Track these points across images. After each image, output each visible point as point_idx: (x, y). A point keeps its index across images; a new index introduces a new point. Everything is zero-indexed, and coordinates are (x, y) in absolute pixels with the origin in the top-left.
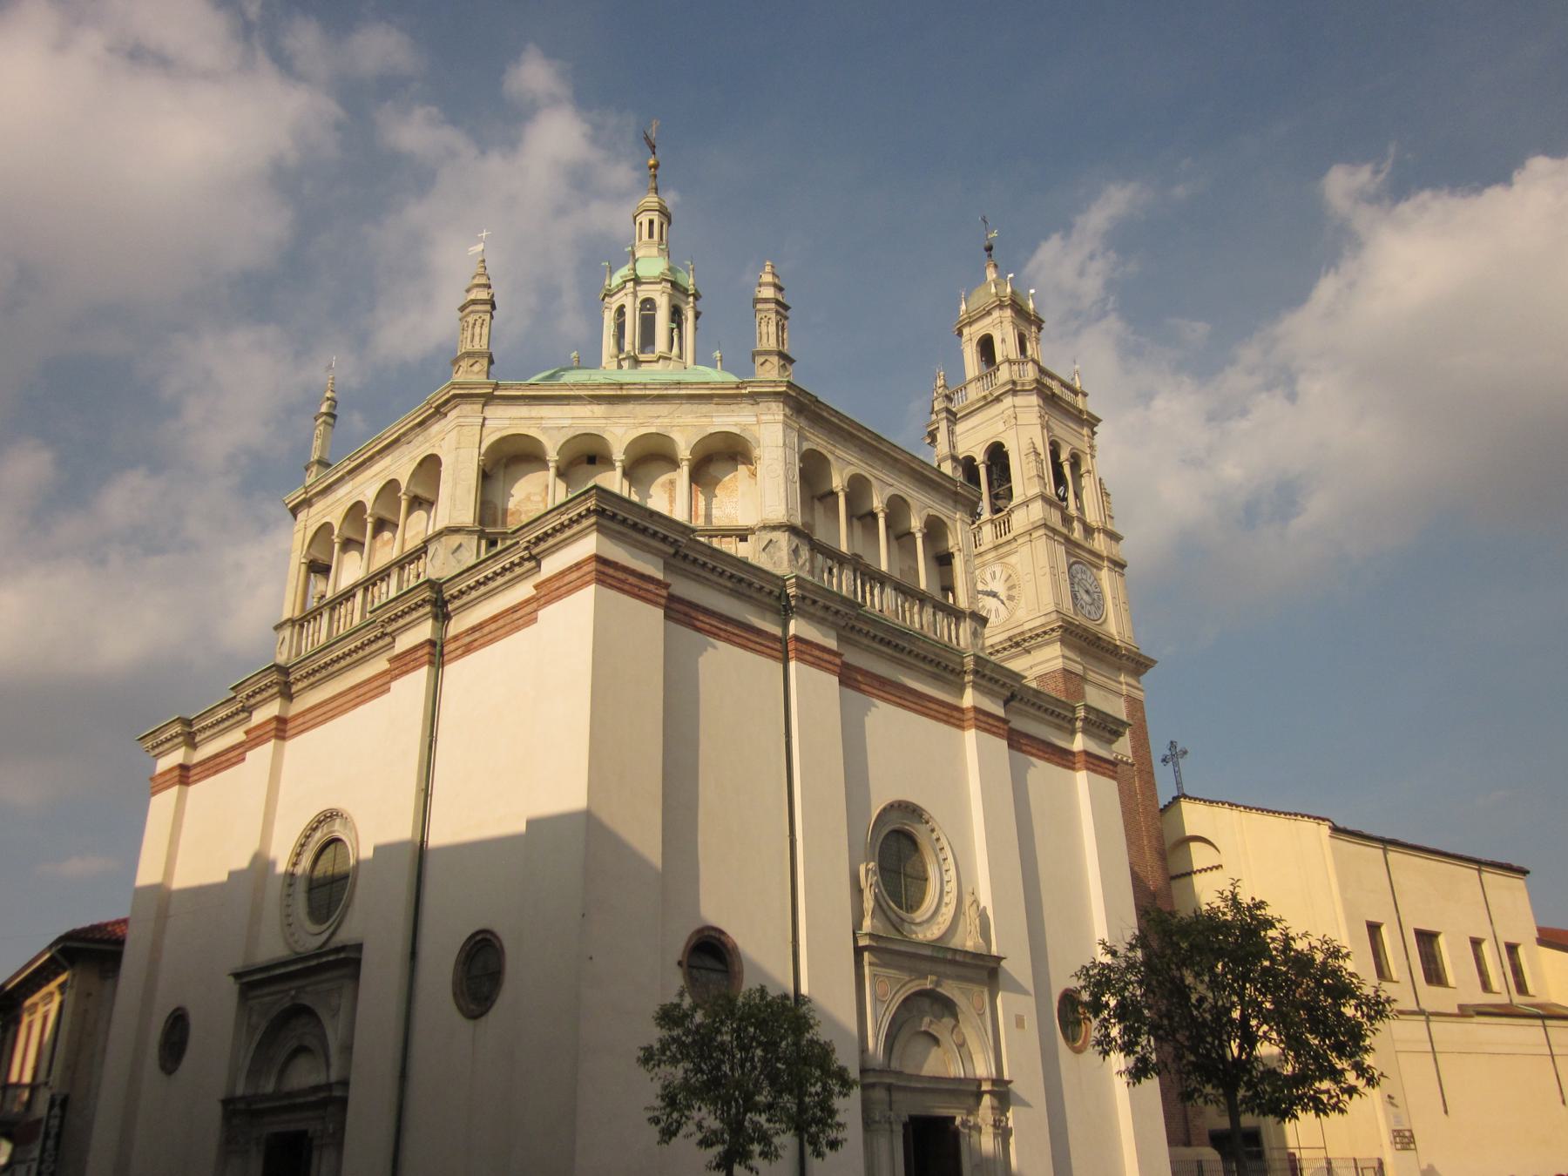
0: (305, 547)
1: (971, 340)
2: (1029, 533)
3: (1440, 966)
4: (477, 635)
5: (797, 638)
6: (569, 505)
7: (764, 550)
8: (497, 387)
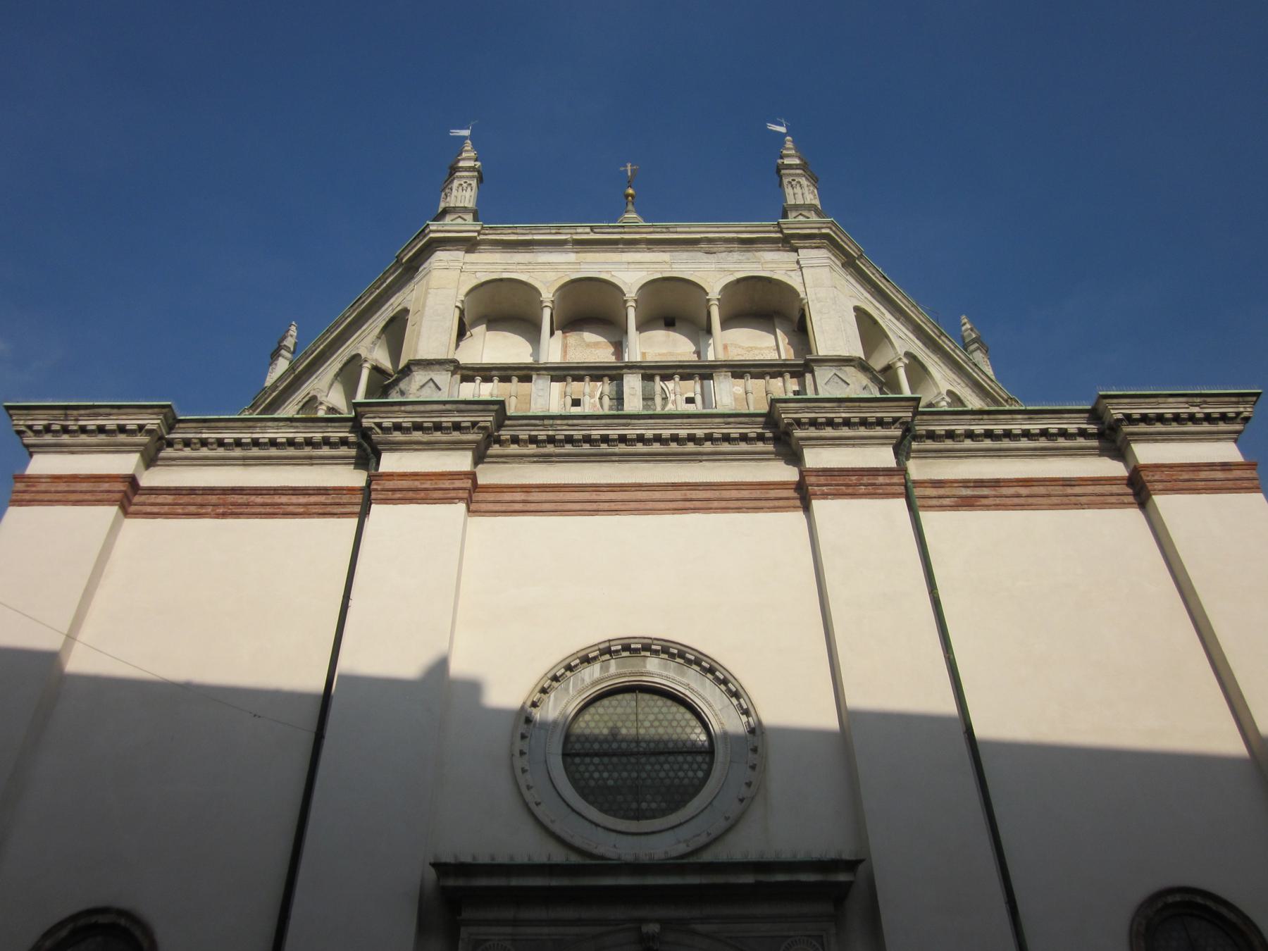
4: (986, 492)
6: (1209, 400)
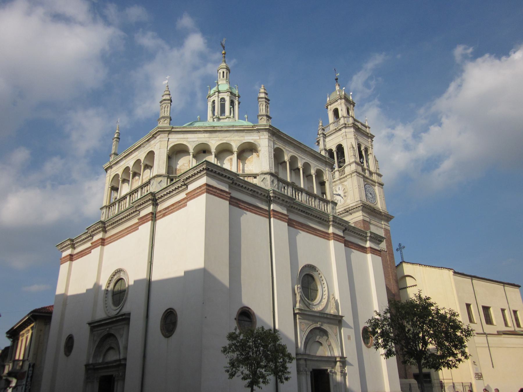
0: (110, 182)
1: (331, 110)
2: (351, 174)
3: (491, 318)
4: (167, 210)
5: (273, 210)
6: (197, 167)
7: (262, 181)
8: (173, 128)
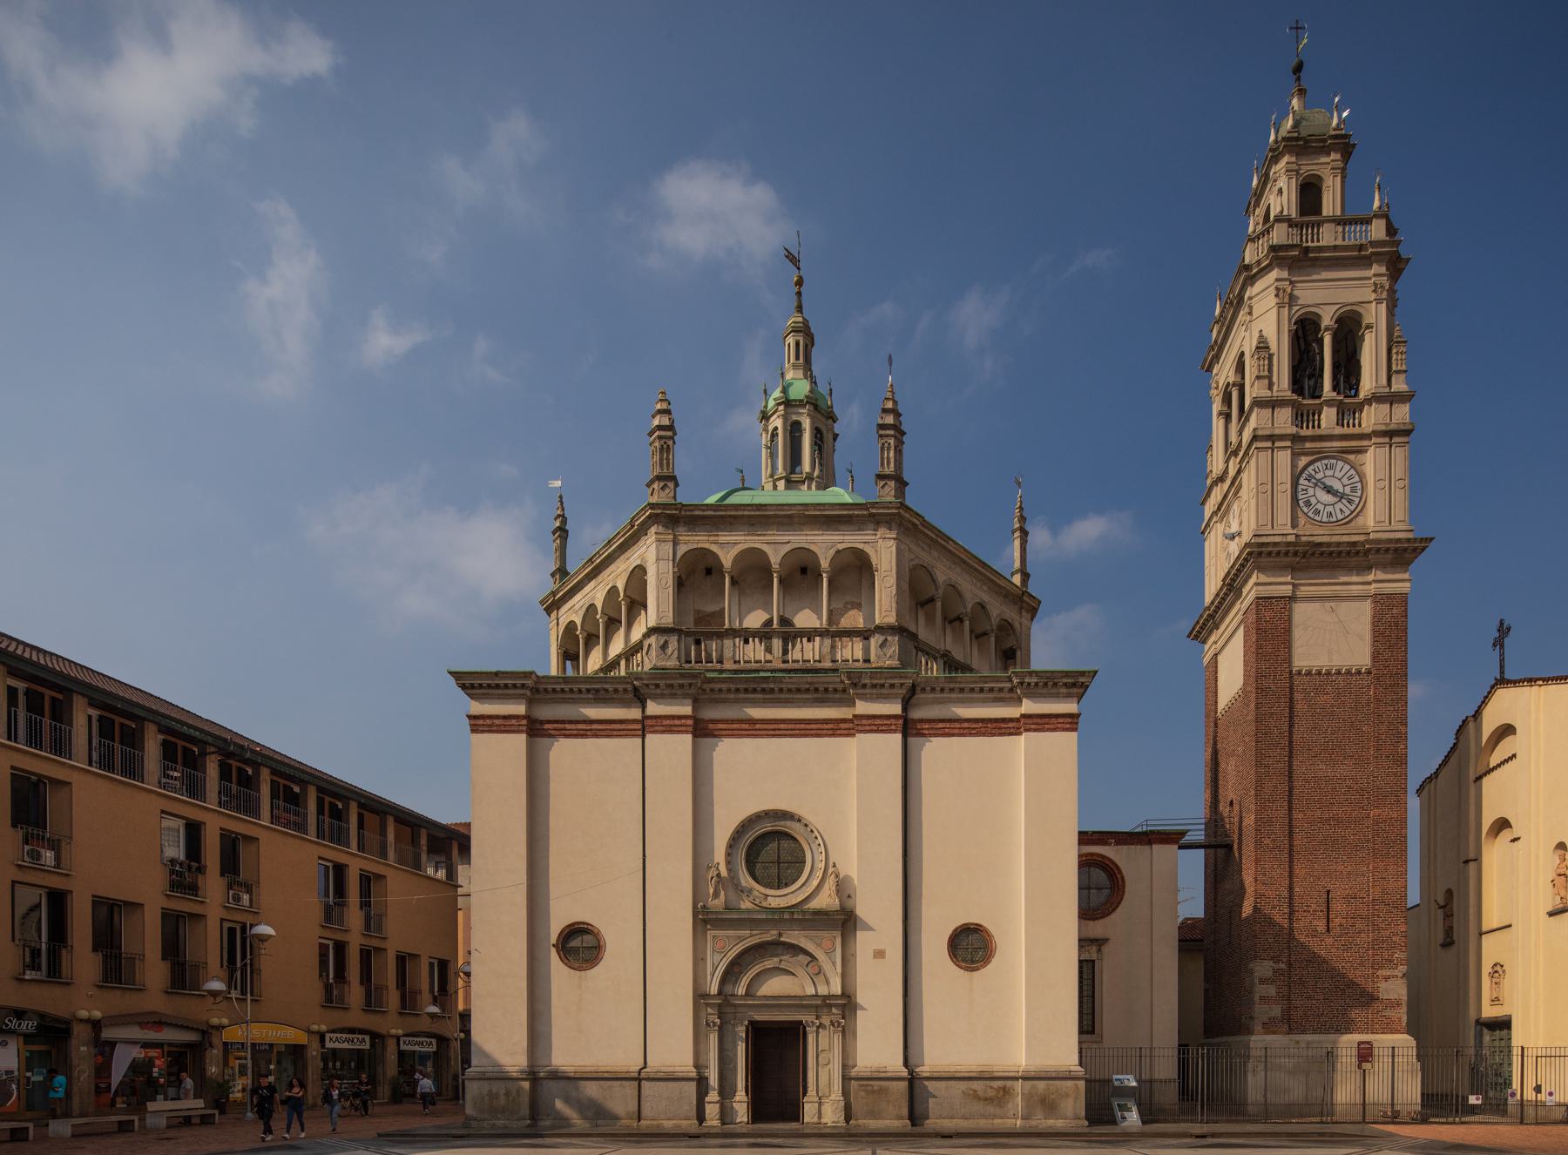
7: (647, 654)
